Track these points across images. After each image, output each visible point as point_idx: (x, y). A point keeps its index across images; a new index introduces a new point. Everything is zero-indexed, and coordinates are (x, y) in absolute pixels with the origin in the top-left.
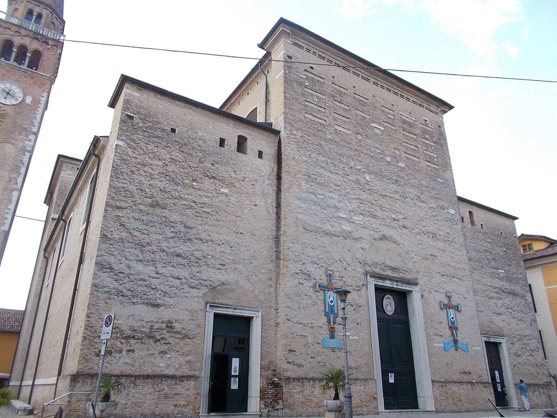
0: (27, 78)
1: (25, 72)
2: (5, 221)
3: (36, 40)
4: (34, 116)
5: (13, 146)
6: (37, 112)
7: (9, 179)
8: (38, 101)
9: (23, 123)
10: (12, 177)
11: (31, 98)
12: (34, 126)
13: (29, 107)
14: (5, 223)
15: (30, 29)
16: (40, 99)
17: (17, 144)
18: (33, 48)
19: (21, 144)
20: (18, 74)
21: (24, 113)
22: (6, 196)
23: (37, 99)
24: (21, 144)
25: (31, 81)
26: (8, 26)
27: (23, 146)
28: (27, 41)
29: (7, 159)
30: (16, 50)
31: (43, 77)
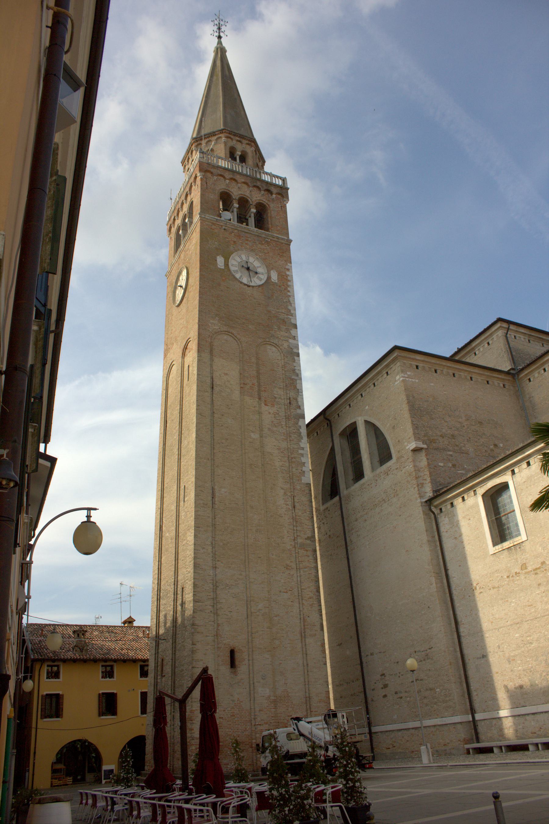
0: (262, 244)
1: (258, 236)
2: (304, 469)
3: (255, 189)
4: (288, 301)
7: (288, 401)
8: (285, 277)
9: (279, 312)
10: (291, 397)
11: (276, 272)
12: (292, 316)
13: (278, 287)
15: (245, 172)
16: (286, 274)
17: (281, 345)
18: (255, 201)
19: (285, 344)
20: (250, 239)
21: (275, 298)
22: (293, 428)
23: (283, 274)
24: (285, 345)
26: (220, 173)
27: (289, 346)
29: (276, 369)
30: (237, 206)
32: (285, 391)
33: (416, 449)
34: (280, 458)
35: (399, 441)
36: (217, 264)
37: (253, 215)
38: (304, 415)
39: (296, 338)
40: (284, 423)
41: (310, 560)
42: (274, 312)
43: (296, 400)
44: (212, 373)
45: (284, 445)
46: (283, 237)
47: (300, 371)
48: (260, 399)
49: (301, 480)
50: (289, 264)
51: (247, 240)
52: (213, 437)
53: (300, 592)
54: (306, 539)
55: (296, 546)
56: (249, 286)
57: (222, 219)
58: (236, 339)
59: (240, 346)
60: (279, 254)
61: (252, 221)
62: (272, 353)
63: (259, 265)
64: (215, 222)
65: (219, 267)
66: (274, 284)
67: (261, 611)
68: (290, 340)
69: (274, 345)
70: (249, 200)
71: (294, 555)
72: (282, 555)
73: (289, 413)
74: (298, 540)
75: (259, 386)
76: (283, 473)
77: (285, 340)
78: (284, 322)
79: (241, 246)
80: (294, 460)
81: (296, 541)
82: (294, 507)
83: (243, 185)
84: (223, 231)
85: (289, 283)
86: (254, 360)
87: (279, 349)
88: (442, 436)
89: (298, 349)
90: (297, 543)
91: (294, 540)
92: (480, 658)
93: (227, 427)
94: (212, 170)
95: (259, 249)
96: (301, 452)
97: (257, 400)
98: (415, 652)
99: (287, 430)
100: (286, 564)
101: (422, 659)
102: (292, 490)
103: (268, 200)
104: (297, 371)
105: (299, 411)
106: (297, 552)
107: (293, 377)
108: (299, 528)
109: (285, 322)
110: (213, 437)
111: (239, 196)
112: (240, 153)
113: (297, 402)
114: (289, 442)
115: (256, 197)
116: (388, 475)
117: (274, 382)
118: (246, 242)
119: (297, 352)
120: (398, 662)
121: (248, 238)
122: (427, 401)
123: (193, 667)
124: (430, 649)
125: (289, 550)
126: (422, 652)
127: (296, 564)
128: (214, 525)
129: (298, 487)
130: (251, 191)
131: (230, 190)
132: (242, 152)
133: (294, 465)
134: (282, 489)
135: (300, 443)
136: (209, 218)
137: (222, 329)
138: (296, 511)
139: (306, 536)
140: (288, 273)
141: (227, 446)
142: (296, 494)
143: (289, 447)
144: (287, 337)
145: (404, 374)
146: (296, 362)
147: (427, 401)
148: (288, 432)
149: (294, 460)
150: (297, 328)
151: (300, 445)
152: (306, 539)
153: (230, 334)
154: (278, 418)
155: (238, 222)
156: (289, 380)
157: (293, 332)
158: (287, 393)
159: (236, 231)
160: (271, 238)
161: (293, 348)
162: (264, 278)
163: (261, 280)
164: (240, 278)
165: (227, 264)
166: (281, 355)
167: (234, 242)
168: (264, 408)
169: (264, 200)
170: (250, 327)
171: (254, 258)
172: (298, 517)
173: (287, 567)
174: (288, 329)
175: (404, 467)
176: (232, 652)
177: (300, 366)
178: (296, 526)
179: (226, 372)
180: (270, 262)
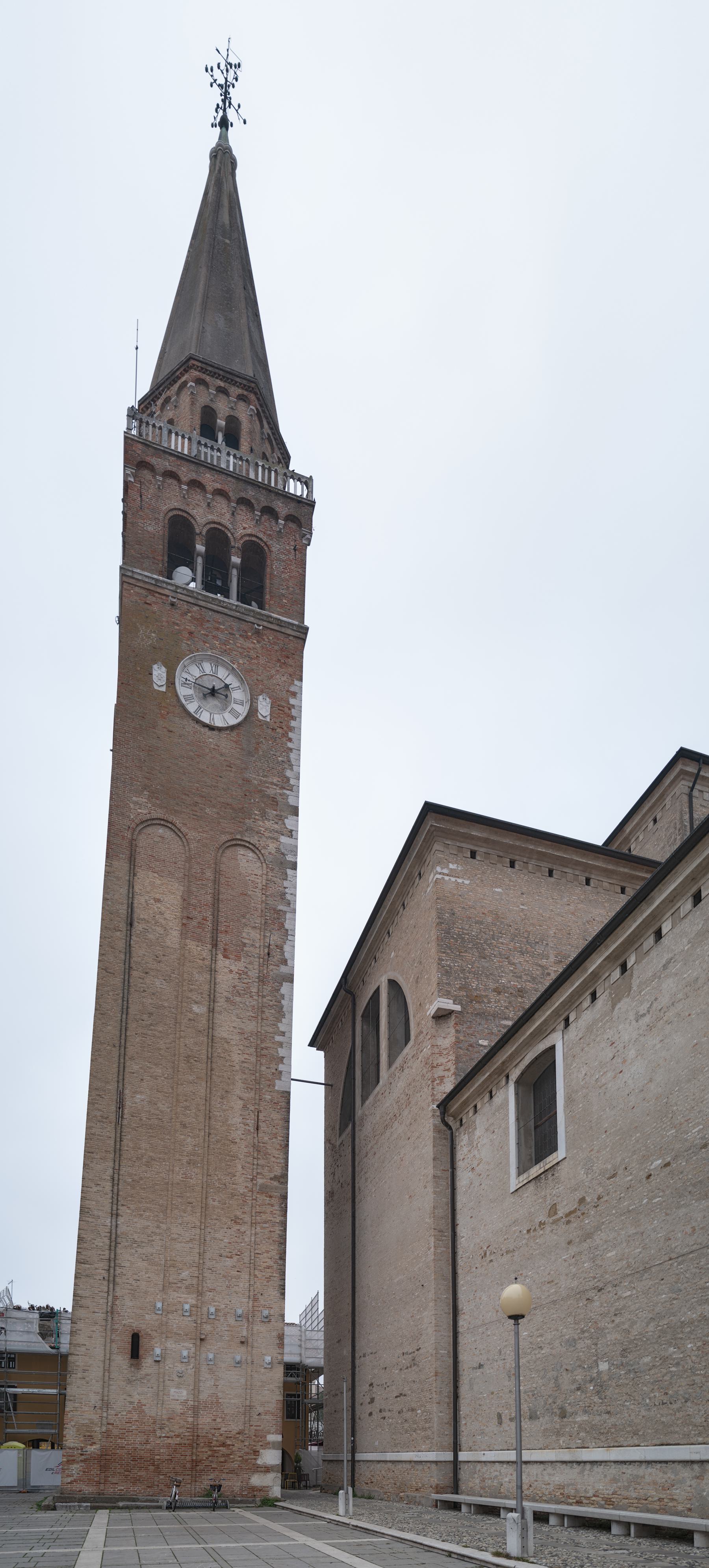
0: (247, 638)
4: (285, 759)
5: (254, 855)
6: (290, 745)
8: (286, 710)
9: (266, 782)
10: (272, 942)
11: (268, 700)
12: (291, 790)
13: (270, 731)
17: (264, 848)
21: (261, 753)
22: (269, 998)
24: (272, 847)
26: (169, 468)
27: (278, 849)
31: (283, 630)
32: (262, 933)
34: (242, 1048)
36: (152, 681)
37: (235, 572)
38: (292, 975)
39: (294, 833)
40: (254, 990)
42: (256, 782)
43: (281, 948)
45: (251, 1026)
46: (290, 621)
47: (295, 896)
48: (215, 945)
49: (274, 1086)
50: (296, 682)
51: (218, 629)
54: (271, 1179)
55: (254, 1189)
56: (212, 728)
58: (180, 835)
59: (187, 848)
60: (279, 660)
62: (245, 861)
64: (152, 588)
65: (156, 687)
66: (262, 724)
68: (282, 837)
69: (251, 846)
70: (229, 535)
72: (231, 1202)
73: (265, 971)
76: (245, 1073)
78: (274, 802)
79: (205, 642)
80: (264, 1052)
82: (257, 1129)
83: (219, 499)
84: (169, 607)
85: (293, 723)
86: (209, 874)
87: (260, 855)
89: (296, 855)
90: (256, 1184)
91: (252, 1180)
93: (153, 994)
94: (153, 461)
95: (240, 650)
96: (278, 1038)
97: (209, 946)
99: (260, 1001)
100: (235, 1216)
102: (257, 1102)
103: (270, 535)
104: (288, 897)
105: (283, 969)
106: (254, 1197)
107: (280, 907)
108: (260, 1162)
109: (277, 802)
111: (208, 526)
113: (283, 953)
114: (260, 1021)
115: (244, 528)
117: (244, 916)
119: (293, 860)
121: (219, 623)
125: (242, 1195)
129: (268, 1097)
130: (233, 514)
131: (190, 512)
133: (264, 1061)
134: (240, 1098)
135: (280, 1025)
136: (140, 578)
138: (259, 1135)
139: (272, 1175)
140: (292, 701)
142: (262, 1108)
143: (259, 1030)
144: (277, 832)
146: (289, 879)
148: (260, 1005)
149: (264, 1052)
150: (297, 815)
151: (278, 1028)
152: (271, 1179)
153: (170, 825)
154: (245, 981)
156: (272, 912)
157: (289, 822)
158: (264, 936)
159: (196, 608)
160: (265, 624)
161: (286, 853)
162: (243, 711)
164: (196, 712)
165: (171, 682)
166: (262, 866)
167: (191, 633)
168: (222, 963)
169: (261, 535)
170: (208, 810)
171: (227, 669)
172: (262, 1145)
173: (236, 1220)
174: (282, 816)
177: (295, 888)
178: (258, 1159)
179: (157, 896)
180: (259, 678)
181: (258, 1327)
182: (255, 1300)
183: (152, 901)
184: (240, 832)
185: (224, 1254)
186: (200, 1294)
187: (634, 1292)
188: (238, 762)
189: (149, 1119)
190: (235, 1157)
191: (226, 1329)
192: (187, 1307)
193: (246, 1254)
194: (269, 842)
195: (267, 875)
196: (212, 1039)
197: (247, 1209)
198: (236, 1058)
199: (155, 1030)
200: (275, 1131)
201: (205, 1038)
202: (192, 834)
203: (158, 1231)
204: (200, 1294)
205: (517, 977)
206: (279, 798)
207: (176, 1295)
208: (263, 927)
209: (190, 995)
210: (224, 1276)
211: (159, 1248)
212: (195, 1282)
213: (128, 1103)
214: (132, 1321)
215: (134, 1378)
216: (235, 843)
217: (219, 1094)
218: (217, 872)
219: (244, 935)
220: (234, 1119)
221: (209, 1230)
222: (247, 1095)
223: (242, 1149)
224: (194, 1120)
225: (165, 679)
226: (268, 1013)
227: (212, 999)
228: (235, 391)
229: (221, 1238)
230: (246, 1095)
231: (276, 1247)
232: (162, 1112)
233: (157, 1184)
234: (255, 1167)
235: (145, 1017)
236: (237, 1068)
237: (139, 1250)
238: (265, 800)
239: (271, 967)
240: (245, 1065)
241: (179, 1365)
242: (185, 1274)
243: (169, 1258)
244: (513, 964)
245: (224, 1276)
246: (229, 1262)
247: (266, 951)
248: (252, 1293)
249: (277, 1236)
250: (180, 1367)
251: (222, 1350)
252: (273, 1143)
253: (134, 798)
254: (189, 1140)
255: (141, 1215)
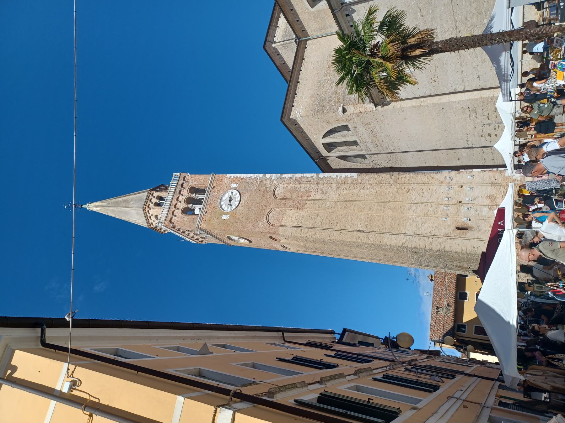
0: (215, 191)
2: (349, 176)
6: (245, 178)
8: (235, 179)
14: (351, 177)
15: (171, 198)
22: (324, 181)
24: (275, 182)
25: (217, 188)
26: (171, 214)
28: (182, 199)
32: (303, 184)
33: (343, 111)
34: (341, 190)
35: (337, 121)
41: (405, 177)
43: (308, 178)
44: (291, 227)
45: (334, 187)
48: (306, 200)
51: (212, 200)
52: (327, 229)
53: (424, 184)
57: (199, 214)
58: (271, 211)
61: (201, 196)
63: (227, 194)
64: (201, 219)
65: (228, 218)
66: (239, 186)
67: (434, 209)
71: (400, 186)
74: (392, 183)
75: (299, 199)
77: (273, 182)
80: (343, 182)
81: (392, 184)
86: (283, 202)
87: (278, 186)
88: (336, 93)
90: (393, 184)
91: (391, 185)
92: (480, 79)
94: (169, 218)
96: (338, 178)
97: (307, 201)
98: (470, 117)
100: (406, 191)
101: (475, 113)
102: (361, 184)
106: (399, 184)
107: (295, 179)
108: (384, 182)
110: (327, 229)
112: (158, 200)
114: (332, 184)
116: (356, 128)
117: (297, 191)
118: (214, 201)
120: (475, 127)
122: (314, 101)
123: (466, 253)
124: (469, 109)
126: (470, 113)
127: (406, 185)
128: (379, 232)
129: (360, 181)
131: (182, 208)
132: (157, 199)
137: (266, 219)
138: (374, 183)
139: (390, 178)
141: (333, 221)
145: (297, 115)
147: (314, 101)
149: (343, 182)
153: (268, 214)
154: (318, 190)
155: (202, 205)
162: (235, 192)
163: (236, 194)
165: (227, 213)
167: (214, 208)
168: (312, 197)
169: (188, 188)
173: (408, 191)
175: (353, 118)
176: (458, 228)
179: (290, 218)
181: (454, 181)
182: (442, 183)
183: (292, 220)
184: (271, 192)
185: (422, 195)
186: (439, 204)
187: (460, 14)
188: (250, 193)
189: (367, 222)
190: (382, 192)
191: (455, 194)
192: (445, 208)
193: (422, 187)
194: (274, 183)
195: (284, 183)
196: (338, 200)
197: (403, 187)
198: (345, 192)
199: (335, 220)
200: (372, 178)
201: (338, 202)
202: (271, 207)
203: (412, 219)
204: (439, 204)
205: (331, 88)
206: (260, 180)
207: (439, 213)
208: (300, 184)
209: (323, 207)
210: (431, 195)
211: (419, 219)
212: (434, 205)
213: (361, 229)
214: (451, 229)
215: (478, 229)
216: (274, 194)
217: (358, 198)
218: (283, 199)
219: (303, 190)
220: (368, 192)
221: (412, 201)
222: (359, 188)
223: (379, 190)
224: (368, 206)
225: (226, 215)
226: (329, 182)
227: (325, 200)
228: (151, 197)
229: (415, 196)
230: (359, 189)
231: (419, 176)
232: (365, 218)
233: (393, 220)
234: (386, 184)
235: (330, 223)
236: (349, 192)
237: (420, 227)
238: (261, 185)
239: (314, 181)
240: (348, 189)
241: (471, 211)
242: (430, 209)
243: (424, 215)
244: (327, 90)
245: (431, 195)
246: (425, 193)
247: (309, 183)
248: (439, 184)
249: (415, 175)
250: (472, 211)
251: (464, 195)
252: (377, 178)
253: (260, 225)
254: (376, 207)
255: (405, 225)
